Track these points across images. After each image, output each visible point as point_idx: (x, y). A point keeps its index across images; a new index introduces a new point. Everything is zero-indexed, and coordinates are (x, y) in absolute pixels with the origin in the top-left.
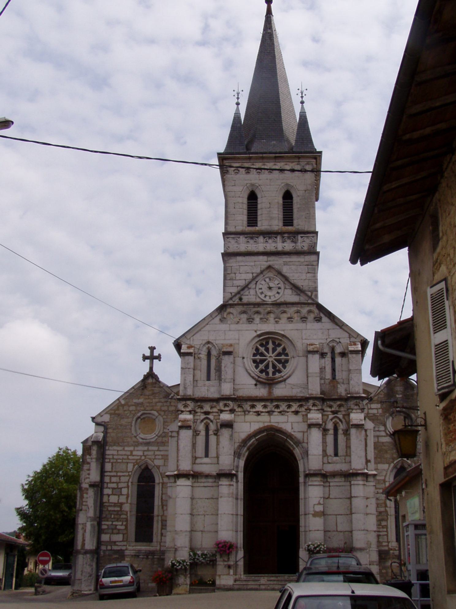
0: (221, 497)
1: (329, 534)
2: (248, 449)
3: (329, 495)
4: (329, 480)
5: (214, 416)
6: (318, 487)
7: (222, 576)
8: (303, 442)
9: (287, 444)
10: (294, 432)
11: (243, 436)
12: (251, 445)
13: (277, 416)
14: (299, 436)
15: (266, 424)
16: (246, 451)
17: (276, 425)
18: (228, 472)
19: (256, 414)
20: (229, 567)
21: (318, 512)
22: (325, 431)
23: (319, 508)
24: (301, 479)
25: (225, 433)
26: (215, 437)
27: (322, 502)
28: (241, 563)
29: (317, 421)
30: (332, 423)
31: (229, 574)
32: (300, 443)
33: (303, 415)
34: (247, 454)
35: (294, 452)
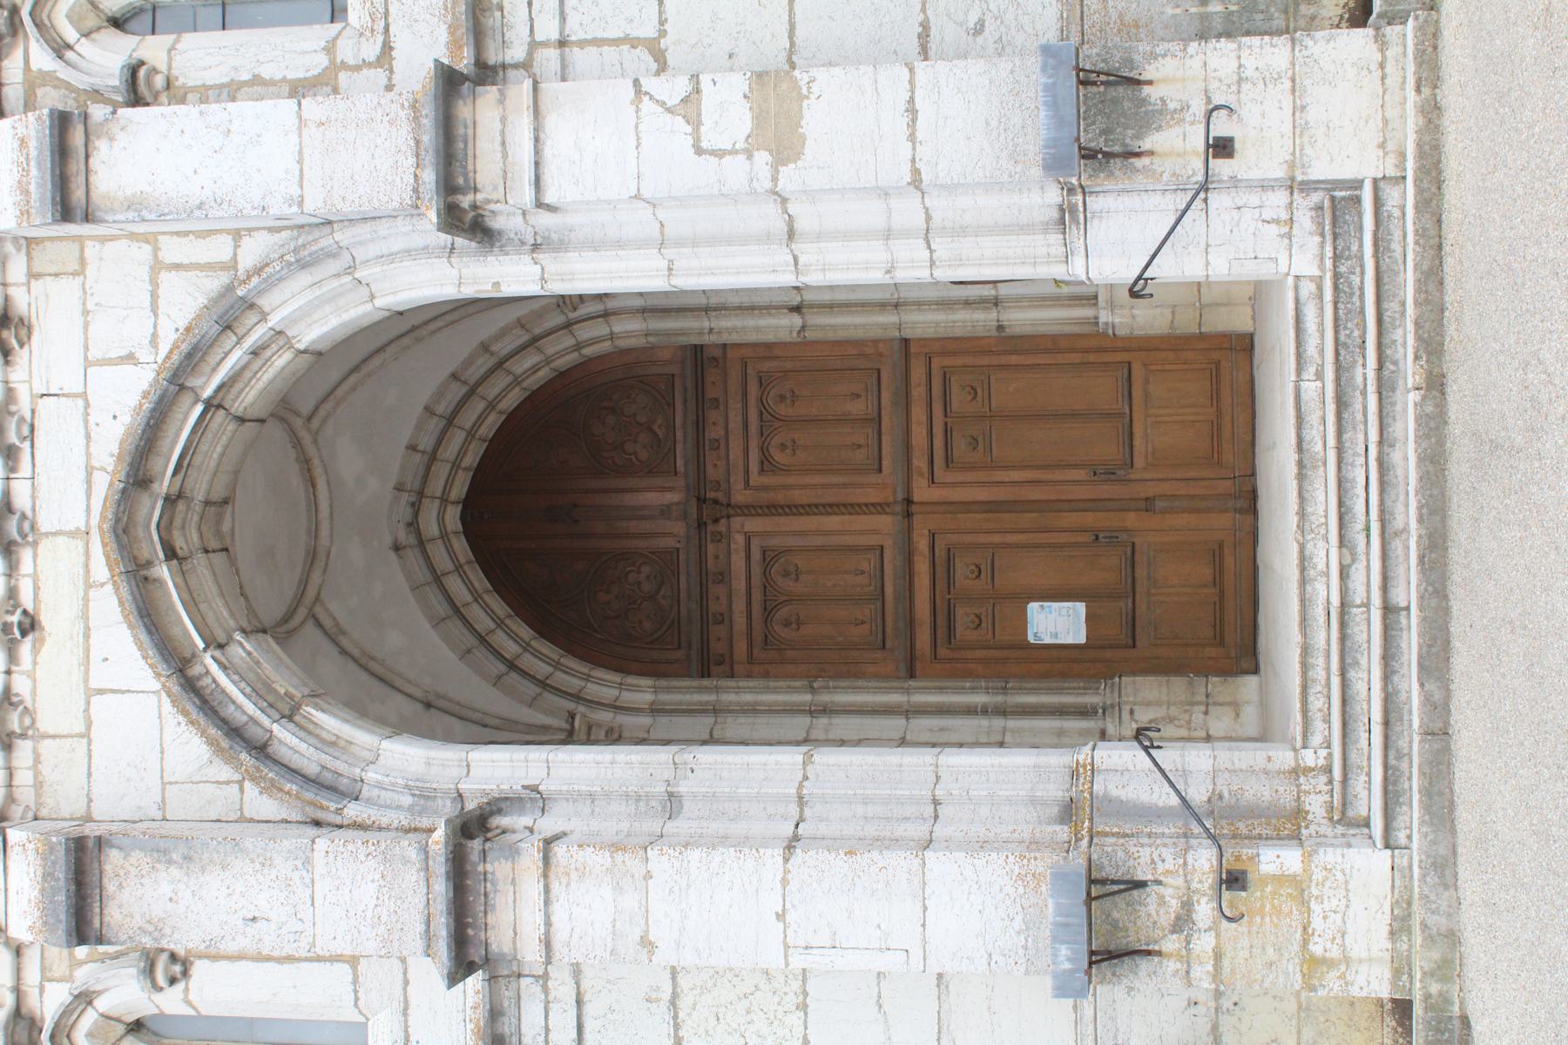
0: (647, 944)
1: (945, 31)
2: (289, 716)
3: (634, 42)
4: (516, 53)
5: (46, 977)
6: (551, 122)
7: (1317, 949)
8: (232, 265)
9: (247, 398)
10: (154, 340)
11: (189, 747)
12: (261, 692)
13: (41, 479)
14: (184, 302)
15: (100, 570)
16: (308, 730)
17: (102, 483)
18: (441, 887)
19: (25, 648)
20: (1234, 880)
21: (760, 118)
22: (136, 89)
23: (729, 111)
24: (510, 276)
25: (136, 896)
26: (199, 968)
27: (672, 88)
28: (1199, 766)
29: (33, 144)
30: (84, 47)
31: (1298, 887)
32: (230, 288)
33: (33, 275)
34: (329, 722)
35: (310, 334)
